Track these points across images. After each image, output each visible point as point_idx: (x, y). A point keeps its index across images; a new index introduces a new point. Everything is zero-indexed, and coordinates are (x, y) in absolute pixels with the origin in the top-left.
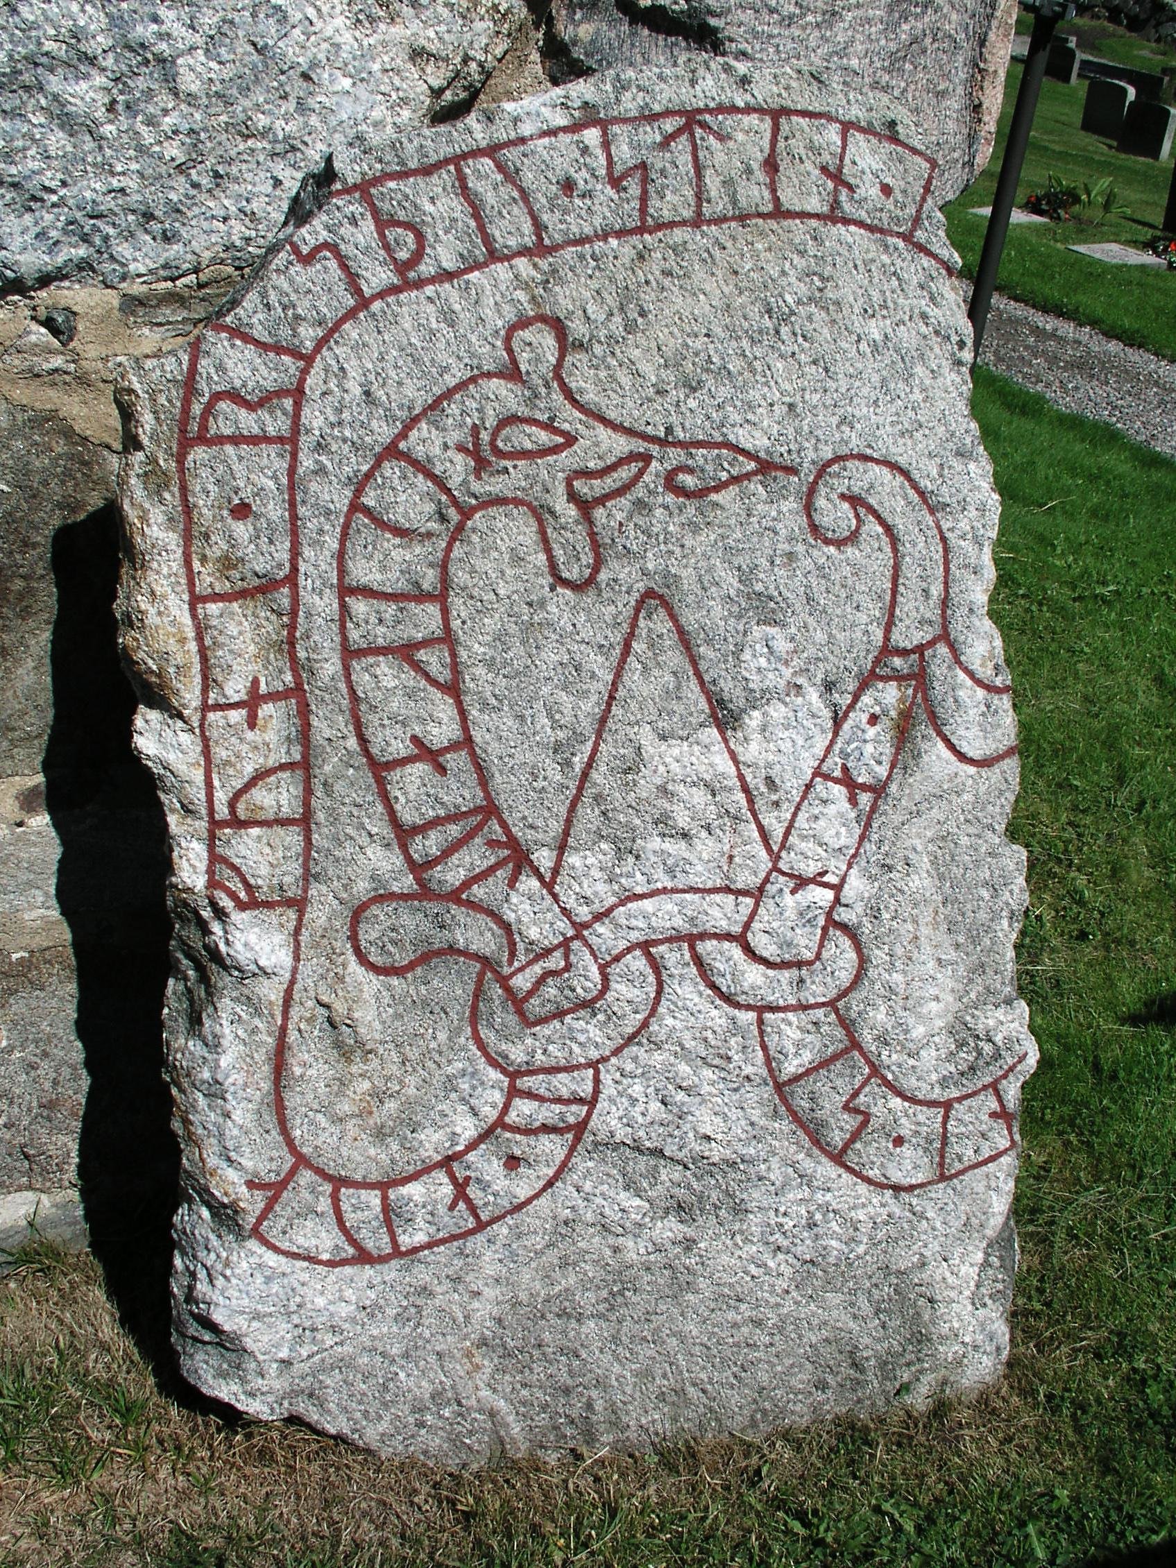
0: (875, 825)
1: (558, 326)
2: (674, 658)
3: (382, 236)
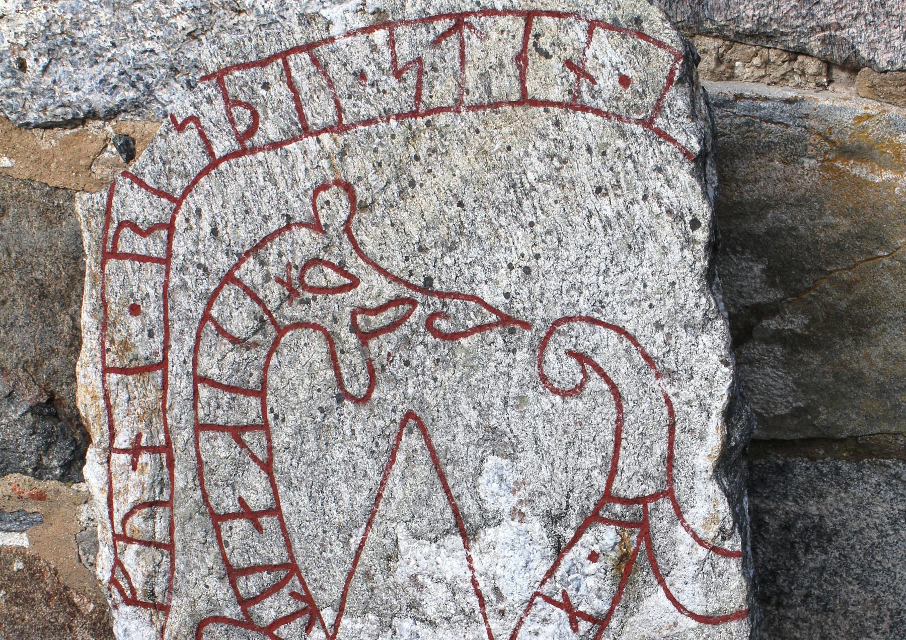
1: (348, 188)
2: (424, 470)
3: (229, 113)
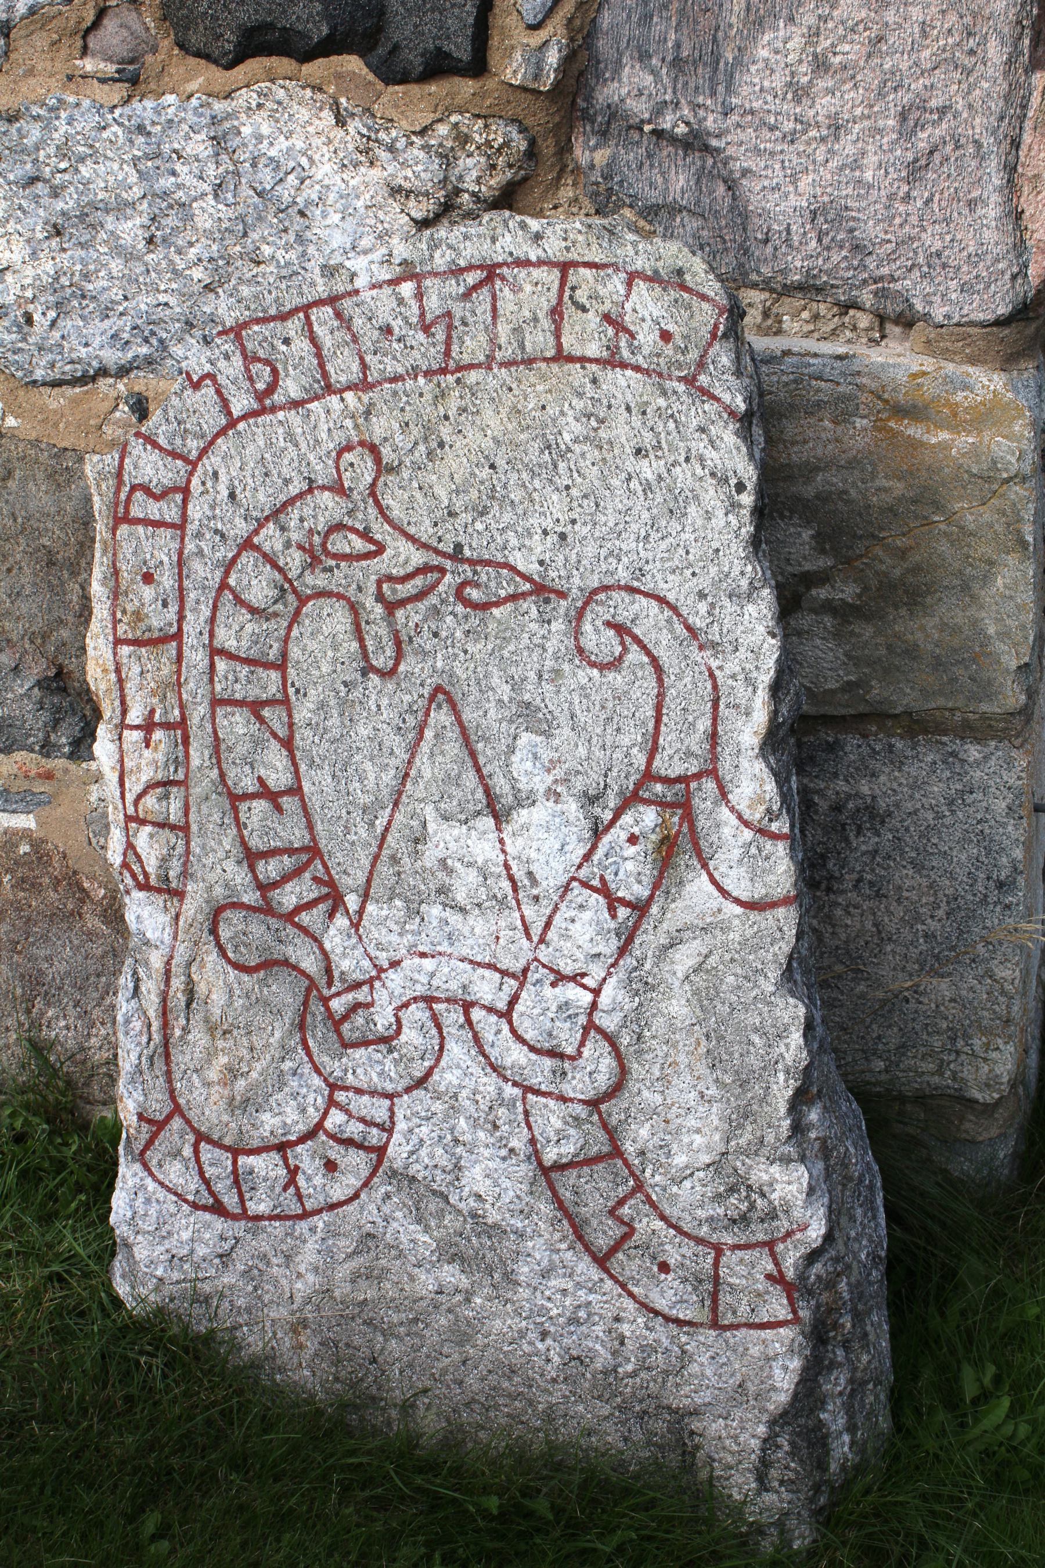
0: (637, 941)
1: (373, 449)
2: (453, 748)
3: (248, 370)
